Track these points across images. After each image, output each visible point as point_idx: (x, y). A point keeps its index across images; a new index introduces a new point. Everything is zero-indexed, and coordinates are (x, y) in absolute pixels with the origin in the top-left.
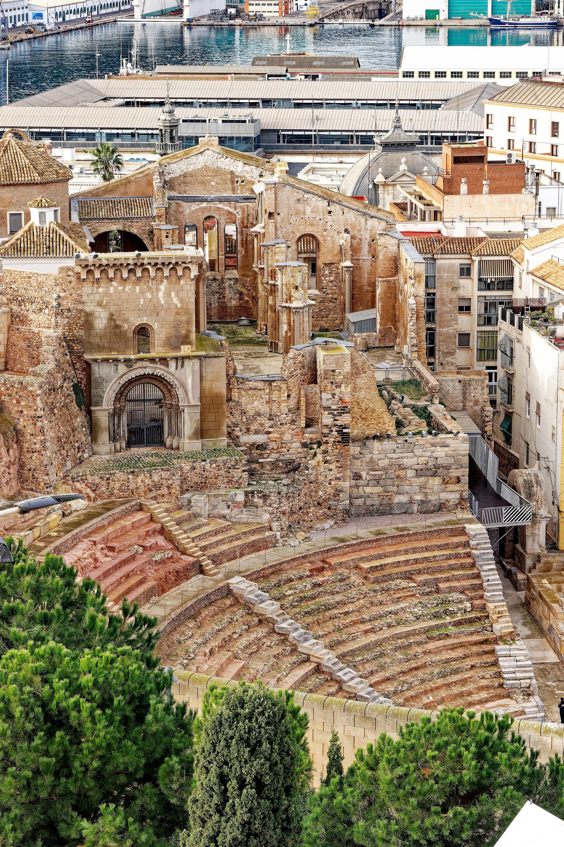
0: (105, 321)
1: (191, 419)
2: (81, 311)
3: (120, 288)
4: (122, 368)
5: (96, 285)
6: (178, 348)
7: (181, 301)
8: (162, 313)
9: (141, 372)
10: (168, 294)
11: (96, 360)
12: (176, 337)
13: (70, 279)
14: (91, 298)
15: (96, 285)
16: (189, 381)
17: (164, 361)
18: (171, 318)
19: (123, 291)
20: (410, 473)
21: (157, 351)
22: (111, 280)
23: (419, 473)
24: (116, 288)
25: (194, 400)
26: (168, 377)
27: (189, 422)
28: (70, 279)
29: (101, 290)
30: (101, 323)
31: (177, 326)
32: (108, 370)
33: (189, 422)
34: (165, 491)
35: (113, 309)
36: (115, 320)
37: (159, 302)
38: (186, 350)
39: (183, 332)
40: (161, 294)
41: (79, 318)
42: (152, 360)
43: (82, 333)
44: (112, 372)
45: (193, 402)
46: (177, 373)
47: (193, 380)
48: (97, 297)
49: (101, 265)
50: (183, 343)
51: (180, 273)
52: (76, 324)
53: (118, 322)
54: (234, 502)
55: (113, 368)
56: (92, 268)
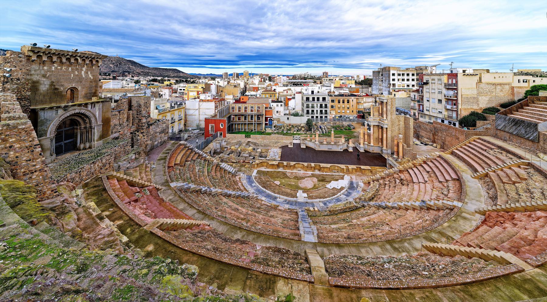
0: (47, 86)
1: (98, 131)
2: (28, 80)
3: (59, 68)
4: (60, 112)
5: (42, 65)
6: (91, 99)
7: (93, 76)
8: (83, 82)
9: (73, 112)
10: (86, 73)
11: (43, 109)
12: (90, 93)
13: (20, 59)
14: (38, 72)
15: (42, 65)
16: (97, 113)
17: (86, 105)
18: (88, 84)
19: (61, 69)
20: (158, 134)
21: (81, 101)
22: (54, 62)
23: (160, 133)
24: (56, 68)
25: (100, 123)
26: (87, 113)
27: (97, 133)
28: (20, 59)
29: (45, 68)
30: (44, 87)
31: (91, 87)
32: (51, 114)
33: (97, 133)
34: (108, 166)
35: (53, 80)
36: (54, 86)
37: (82, 76)
38: (94, 99)
39: (94, 91)
40: (83, 72)
41: (27, 85)
42: (80, 105)
43: (29, 93)
44: (54, 115)
45: (99, 123)
46: (92, 111)
47: (99, 113)
48: (43, 72)
49: (49, 53)
50: (93, 96)
51: (94, 62)
52: (24, 88)
53: (57, 87)
54: (131, 160)
55: (54, 112)
56: (41, 54)
